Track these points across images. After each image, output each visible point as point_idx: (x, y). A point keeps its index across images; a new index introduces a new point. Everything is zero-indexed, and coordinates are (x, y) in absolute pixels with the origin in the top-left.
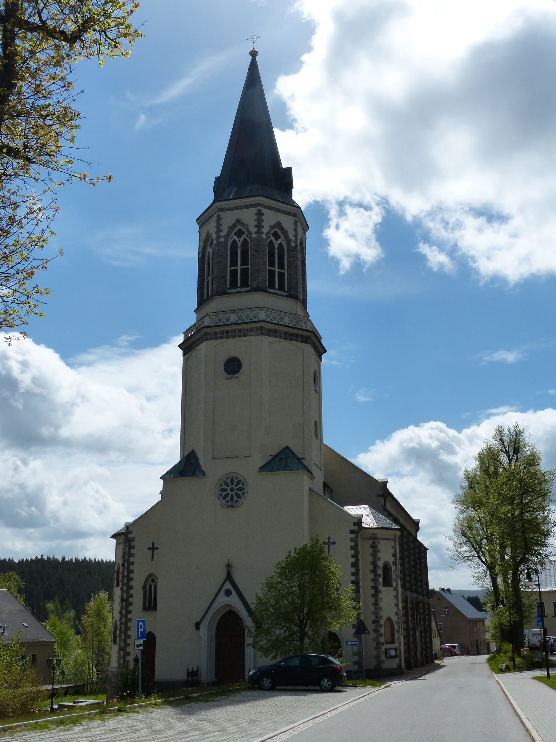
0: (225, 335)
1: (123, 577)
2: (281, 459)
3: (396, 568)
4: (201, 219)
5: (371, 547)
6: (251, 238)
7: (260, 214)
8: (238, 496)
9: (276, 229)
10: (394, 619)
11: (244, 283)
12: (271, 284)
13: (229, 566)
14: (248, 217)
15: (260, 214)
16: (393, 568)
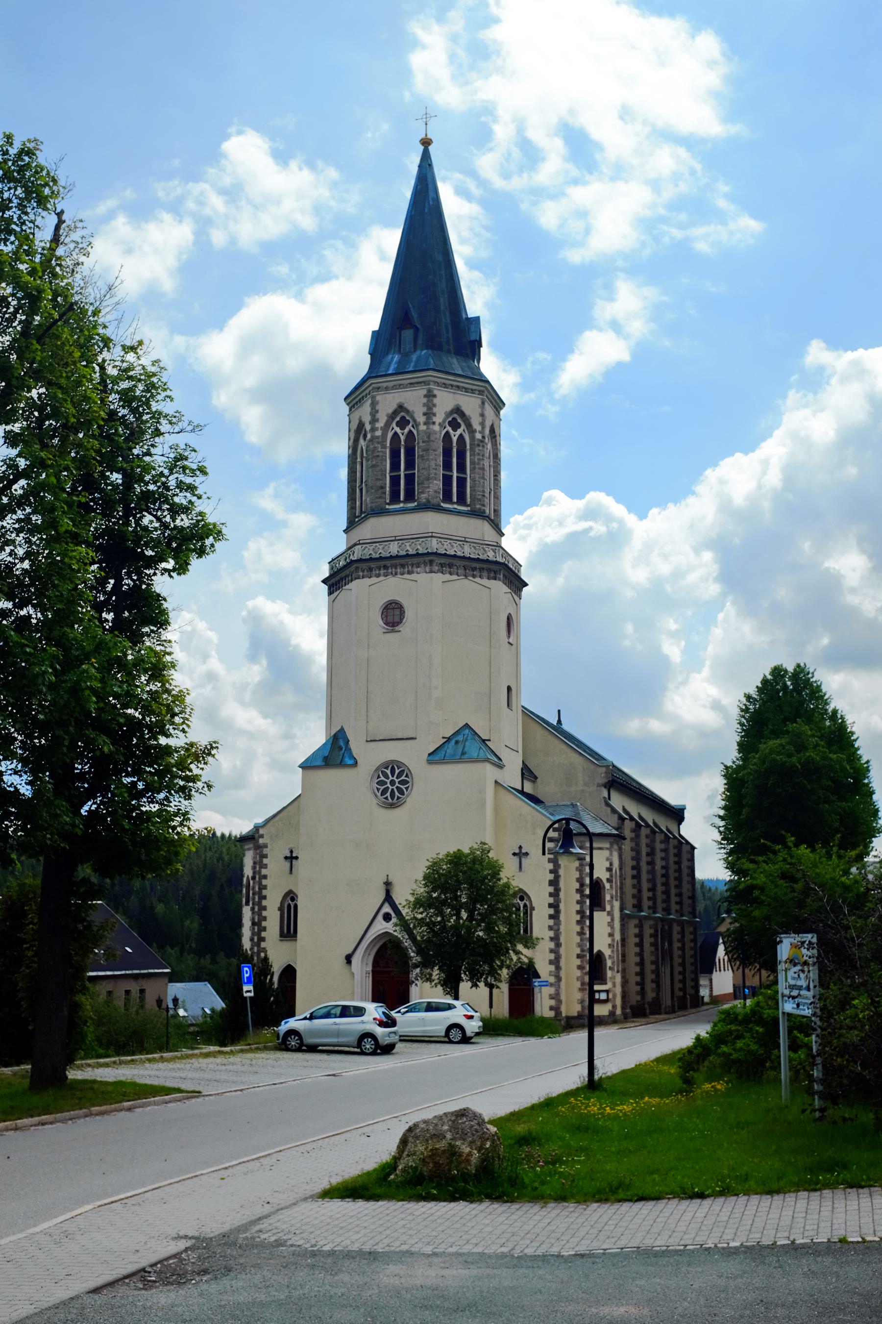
1: (254, 894)
2: (457, 742)
3: (611, 887)
7: (430, 395)
8: (401, 792)
9: (455, 415)
10: (607, 952)
11: (410, 496)
13: (388, 884)
14: (414, 399)
15: (430, 395)
16: (607, 886)
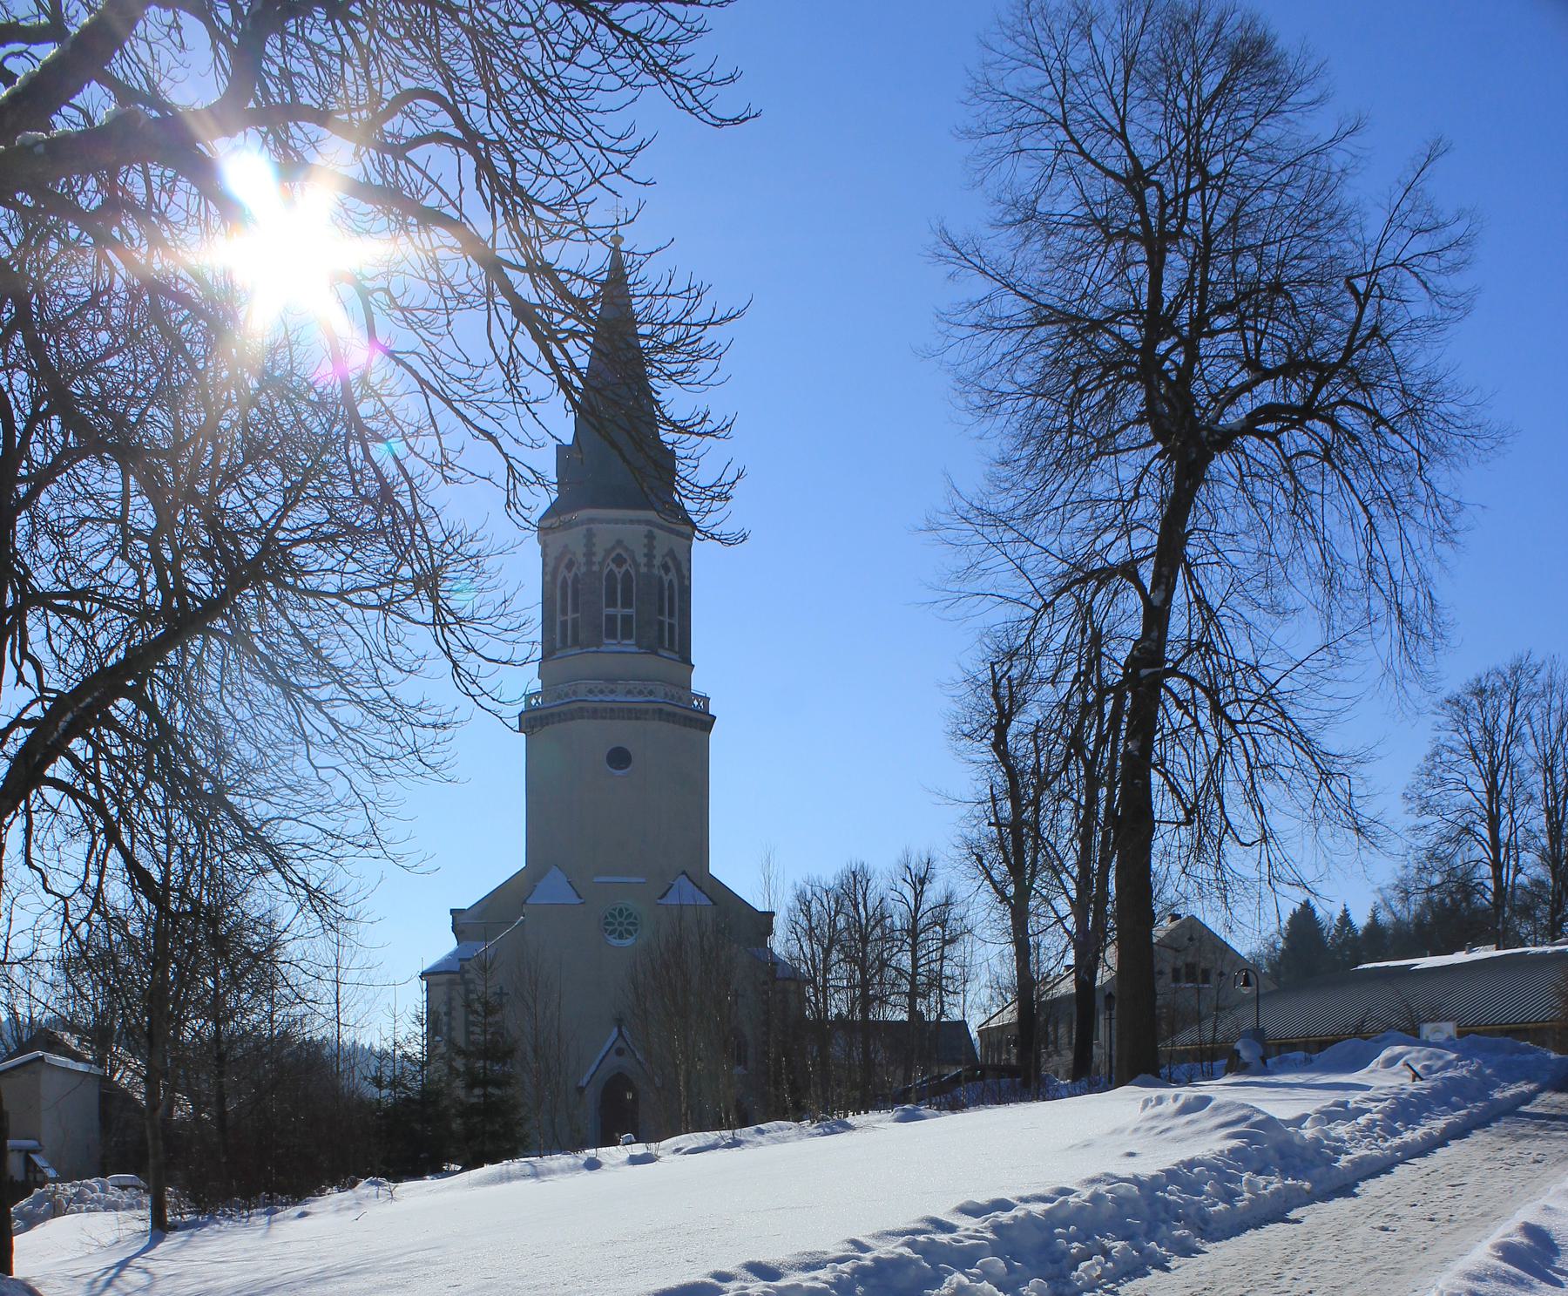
6: (637, 571)
7: (650, 536)
15: (650, 536)
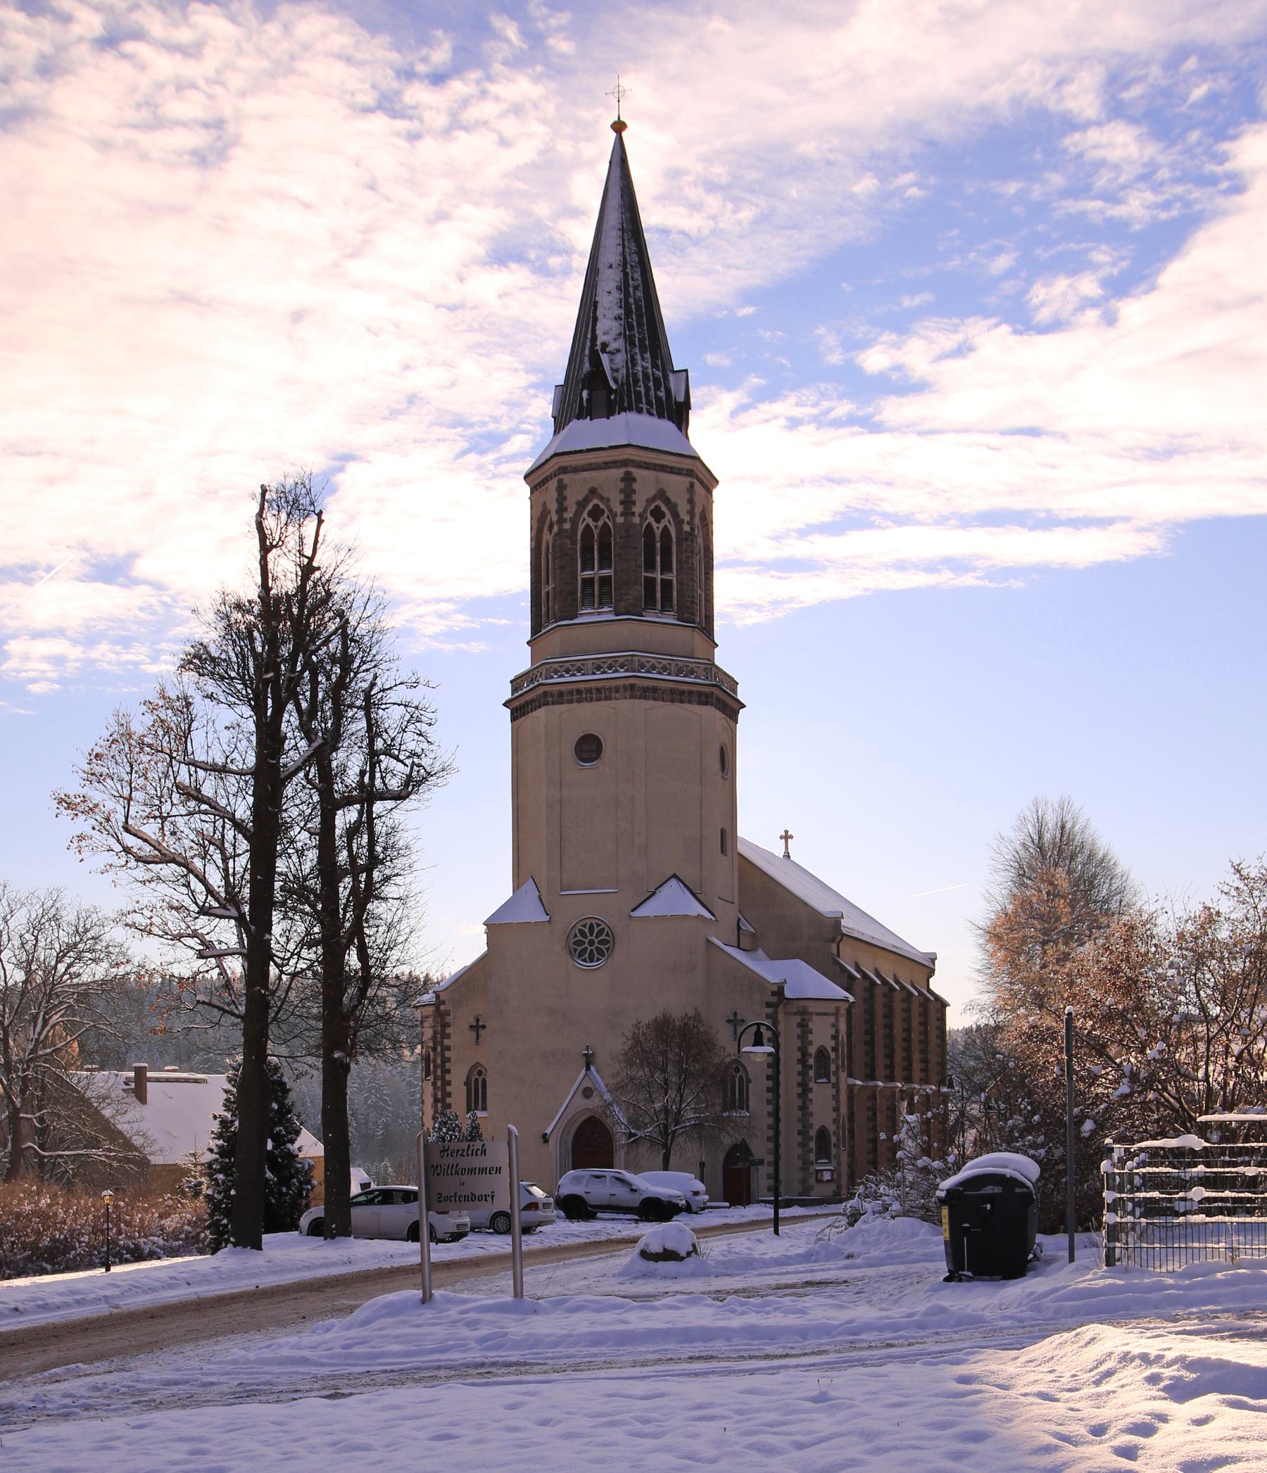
0: (575, 697)
1: (435, 1067)
3: (837, 1056)
4: (534, 476)
5: (799, 1025)
6: (614, 523)
7: (629, 479)
9: (659, 503)
10: (832, 1128)
12: (653, 597)
16: (833, 1055)
